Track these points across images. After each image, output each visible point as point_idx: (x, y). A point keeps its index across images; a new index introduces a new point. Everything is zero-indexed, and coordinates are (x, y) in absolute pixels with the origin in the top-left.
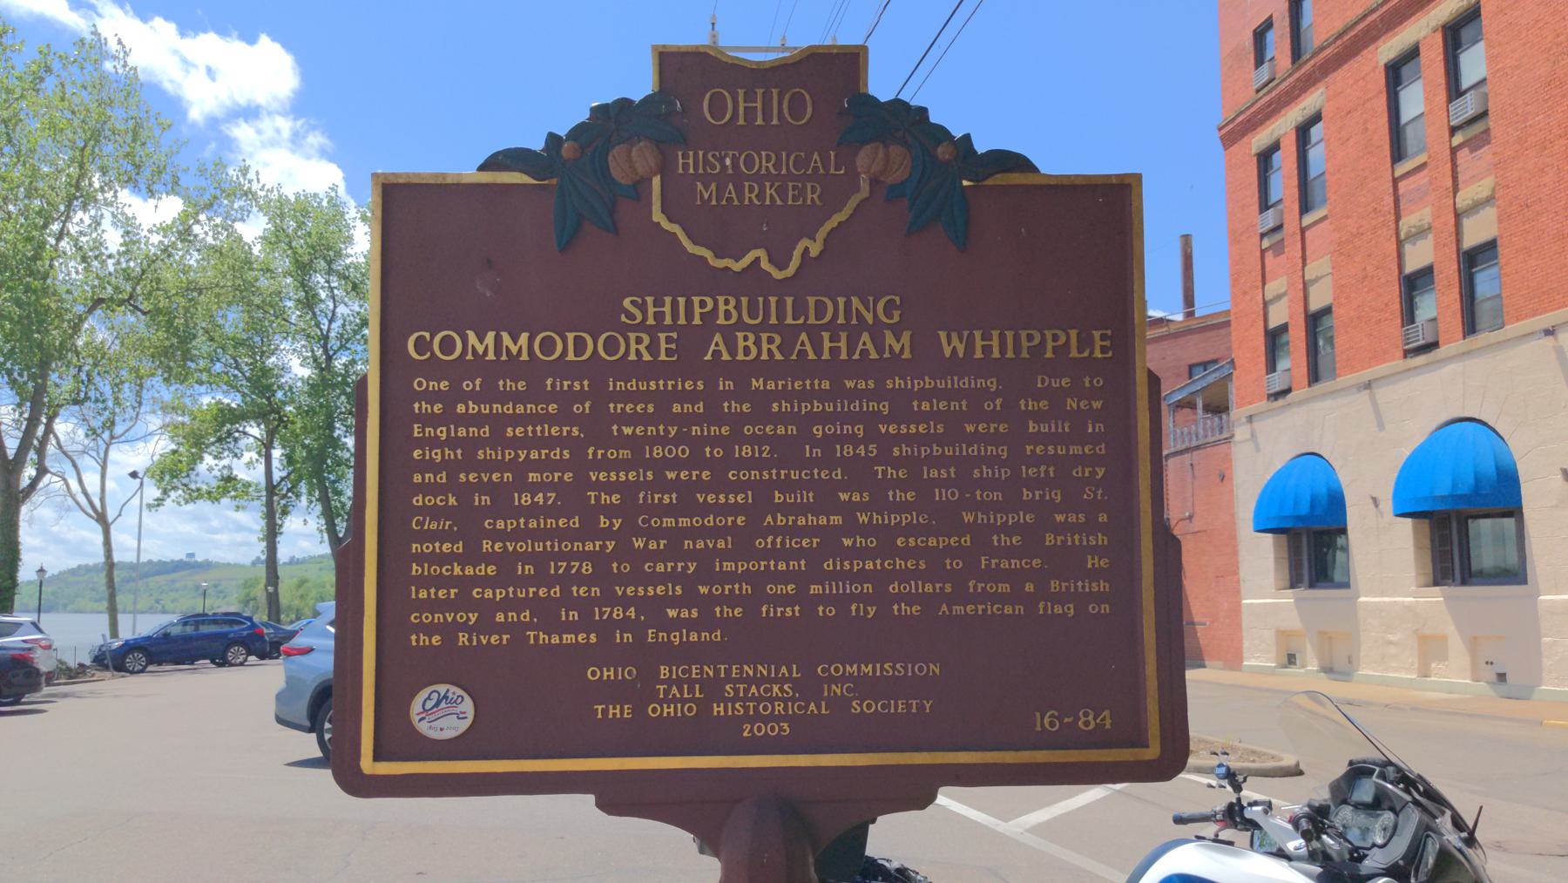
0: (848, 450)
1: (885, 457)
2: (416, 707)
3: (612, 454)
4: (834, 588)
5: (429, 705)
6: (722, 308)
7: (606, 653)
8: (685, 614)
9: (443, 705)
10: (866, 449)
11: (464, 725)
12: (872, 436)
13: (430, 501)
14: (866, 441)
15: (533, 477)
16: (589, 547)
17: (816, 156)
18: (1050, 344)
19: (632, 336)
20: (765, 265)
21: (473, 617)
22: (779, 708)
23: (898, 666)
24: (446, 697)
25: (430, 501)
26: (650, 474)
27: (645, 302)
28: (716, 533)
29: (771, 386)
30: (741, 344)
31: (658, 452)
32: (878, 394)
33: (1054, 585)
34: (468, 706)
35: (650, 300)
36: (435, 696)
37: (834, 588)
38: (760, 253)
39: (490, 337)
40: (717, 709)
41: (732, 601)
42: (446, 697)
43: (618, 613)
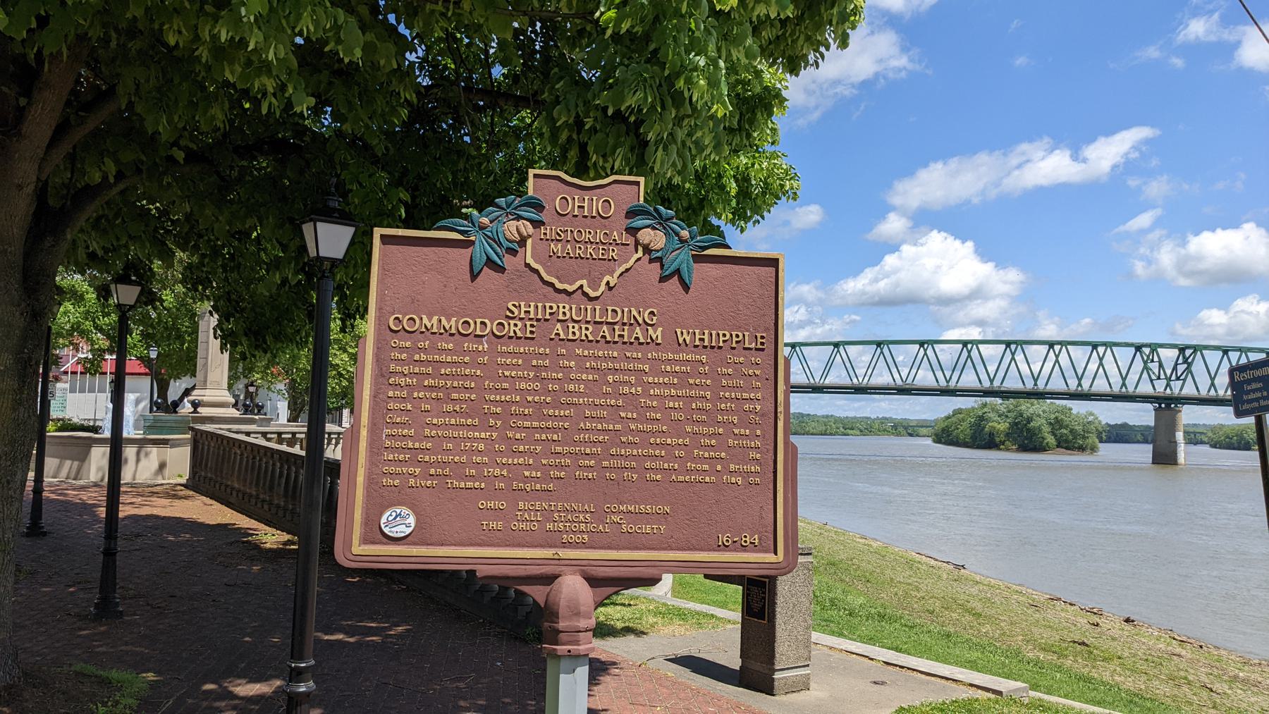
0: (626, 390)
1: (646, 393)
2: (383, 520)
3: (498, 385)
4: (614, 462)
5: (390, 518)
6: (561, 310)
7: (495, 493)
8: (534, 474)
9: (398, 519)
10: (636, 390)
11: (408, 531)
12: (640, 382)
13: (398, 406)
14: (635, 385)
15: (455, 396)
16: (483, 435)
17: (615, 233)
18: (735, 339)
19: (512, 322)
20: (586, 289)
21: (418, 470)
22: (583, 526)
23: (647, 507)
24: (400, 514)
25: (398, 406)
26: (518, 397)
27: (520, 306)
28: (554, 430)
29: (586, 353)
30: (571, 330)
31: (523, 385)
32: (645, 360)
33: (732, 466)
34: (412, 520)
35: (522, 304)
36: (394, 514)
37: (614, 462)
38: (584, 282)
39: (435, 318)
40: (549, 526)
41: (561, 467)
42: (400, 514)
43: (497, 472)
